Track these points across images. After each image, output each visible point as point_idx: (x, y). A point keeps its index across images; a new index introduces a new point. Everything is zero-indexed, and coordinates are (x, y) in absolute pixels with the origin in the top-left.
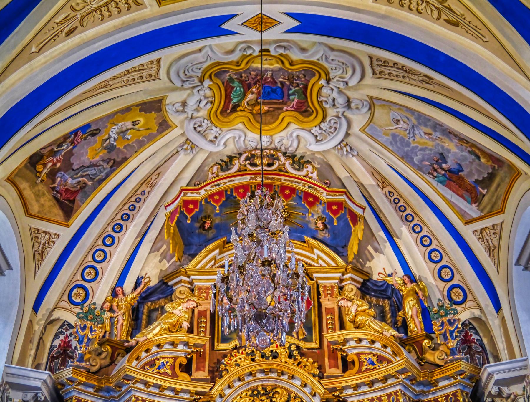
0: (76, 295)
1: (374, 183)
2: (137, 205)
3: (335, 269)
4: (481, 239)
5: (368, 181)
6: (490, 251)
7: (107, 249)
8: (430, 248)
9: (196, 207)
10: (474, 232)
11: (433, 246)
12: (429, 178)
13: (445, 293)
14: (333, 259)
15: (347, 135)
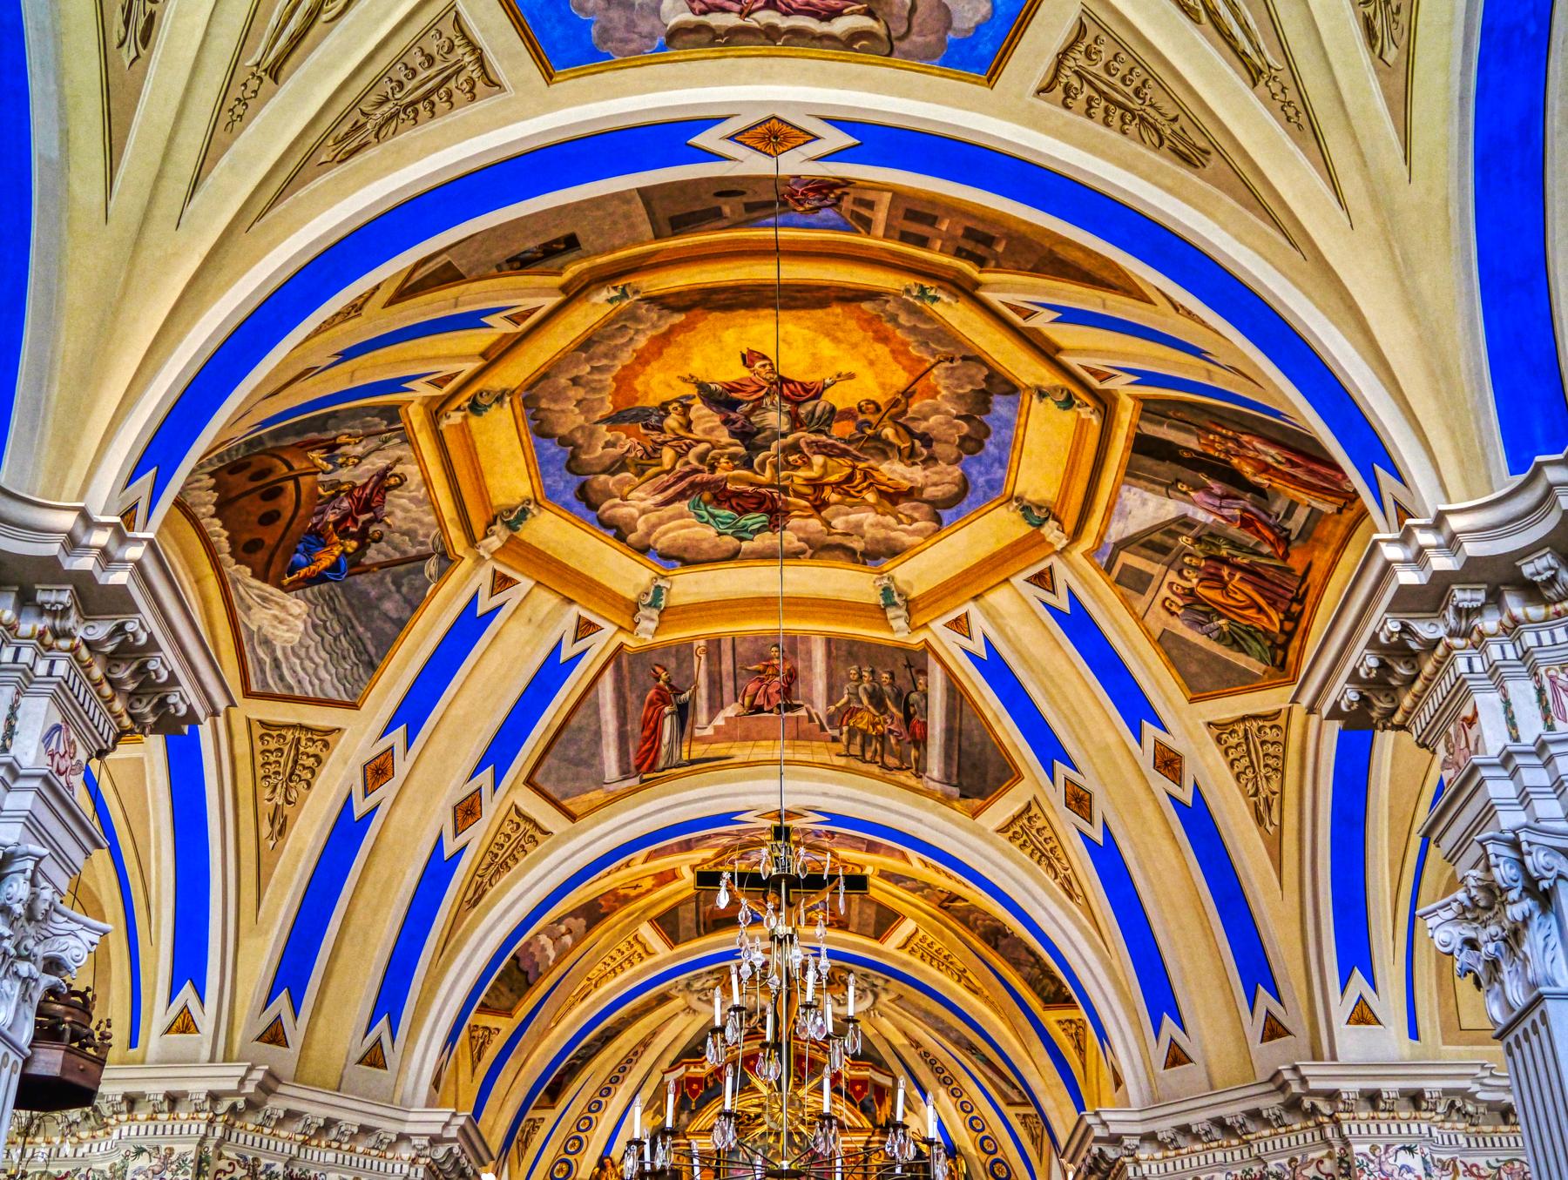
0: (559, 1171)
1: (906, 1042)
2: (628, 1066)
3: (860, 1130)
4: (1024, 1124)
5: (899, 1040)
6: (1034, 1139)
7: (593, 1116)
8: (971, 1115)
9: (700, 1088)
10: (1017, 1115)
11: (975, 1114)
12: (968, 1053)
13: (988, 1166)
14: (859, 1118)
15: (874, 1003)
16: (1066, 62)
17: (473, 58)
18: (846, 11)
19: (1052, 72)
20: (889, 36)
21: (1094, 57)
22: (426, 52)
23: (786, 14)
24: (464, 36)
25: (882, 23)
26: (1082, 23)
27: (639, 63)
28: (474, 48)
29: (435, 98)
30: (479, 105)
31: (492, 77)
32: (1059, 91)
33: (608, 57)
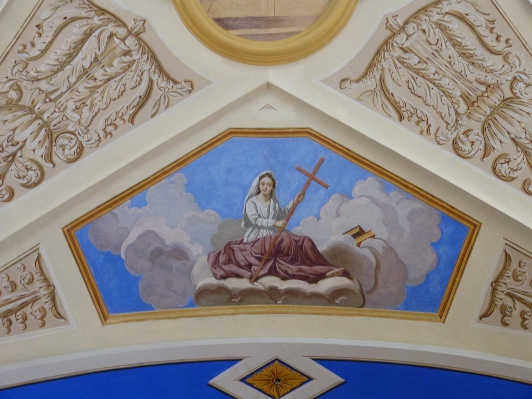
16: (499, 288)
17: (46, 292)
18: (328, 274)
19: (489, 298)
20: (361, 291)
21: (520, 278)
22: (11, 279)
23: (284, 279)
24: (42, 273)
25: (355, 280)
26: (506, 253)
27: (173, 315)
28: (49, 285)
29: (13, 318)
30: (46, 332)
31: (60, 310)
32: (497, 314)
33: (152, 308)
